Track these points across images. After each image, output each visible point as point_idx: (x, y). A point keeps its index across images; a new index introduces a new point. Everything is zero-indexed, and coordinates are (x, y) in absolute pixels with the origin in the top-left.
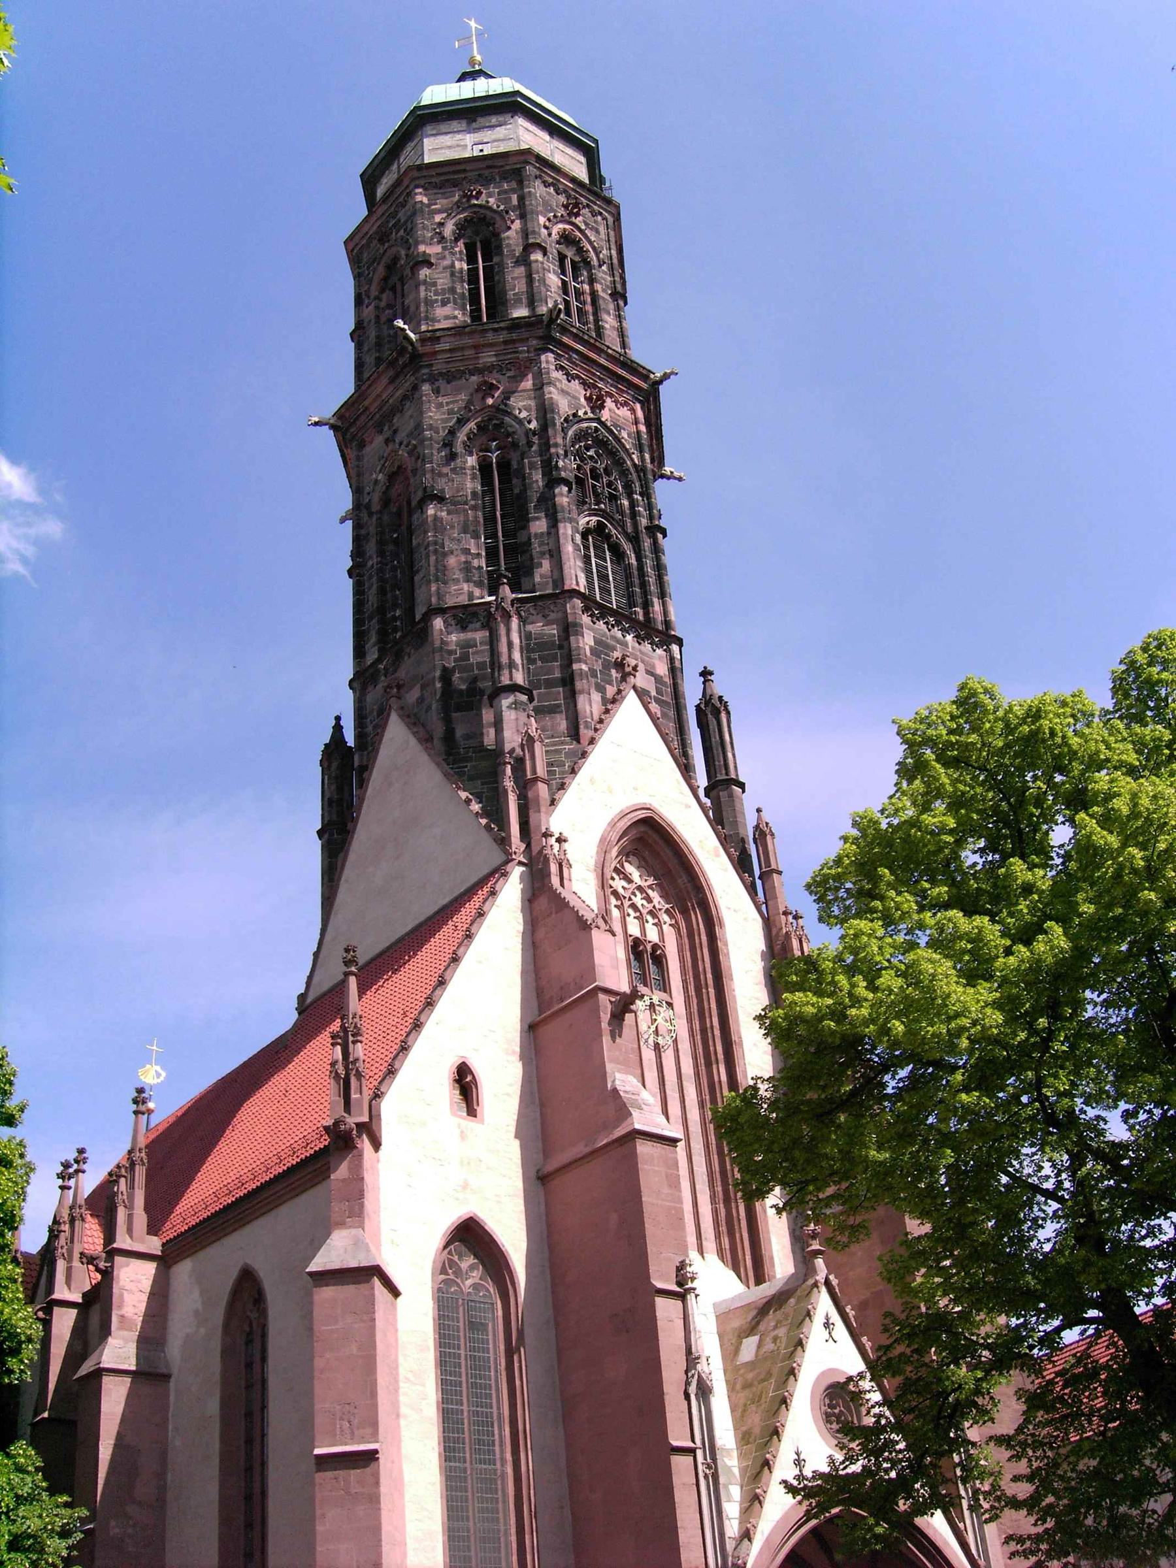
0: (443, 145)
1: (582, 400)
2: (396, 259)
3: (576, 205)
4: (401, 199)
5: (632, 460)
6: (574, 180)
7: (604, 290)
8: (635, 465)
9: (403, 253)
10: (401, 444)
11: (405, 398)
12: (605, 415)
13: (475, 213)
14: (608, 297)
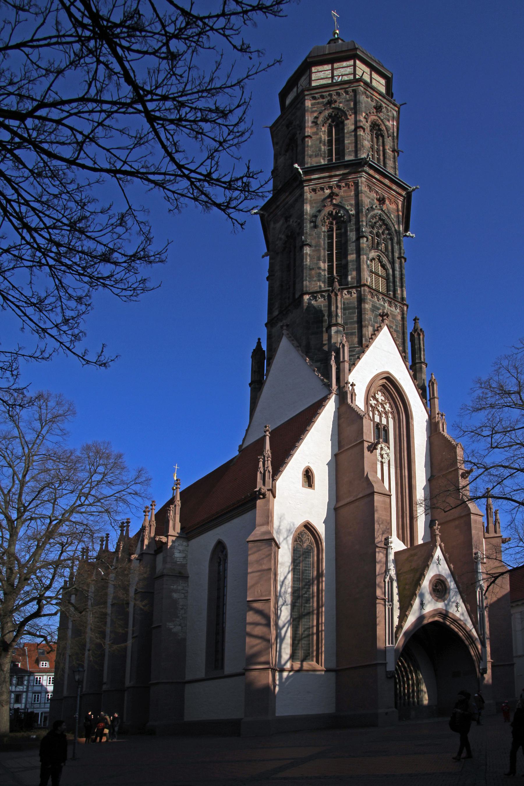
1: (375, 201)
4: (299, 106)
5: (395, 228)
6: (380, 94)
7: (389, 150)
8: (395, 230)
9: (298, 132)
10: (293, 222)
11: (296, 200)
12: (384, 208)
14: (391, 152)
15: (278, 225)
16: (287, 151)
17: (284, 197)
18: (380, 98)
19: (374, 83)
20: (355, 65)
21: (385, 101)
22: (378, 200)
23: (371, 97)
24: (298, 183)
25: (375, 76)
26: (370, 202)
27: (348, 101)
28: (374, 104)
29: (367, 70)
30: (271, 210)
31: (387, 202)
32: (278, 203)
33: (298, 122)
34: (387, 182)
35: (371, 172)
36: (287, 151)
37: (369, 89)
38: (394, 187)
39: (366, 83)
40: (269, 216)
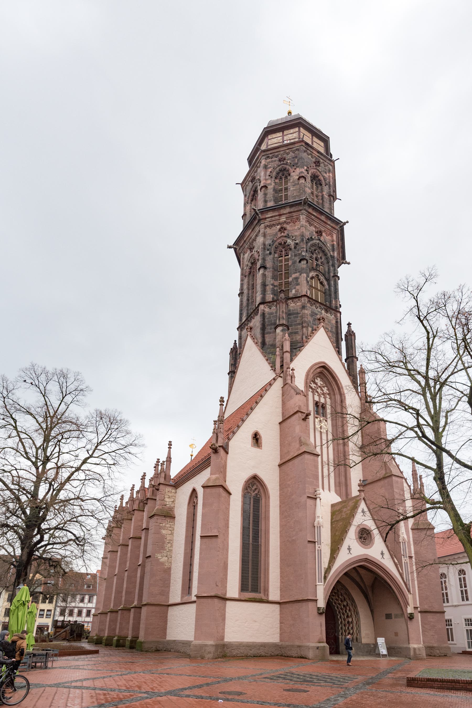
0: (274, 143)
1: (314, 233)
2: (256, 188)
3: (319, 162)
13: (282, 167)
15: (246, 255)
16: (252, 200)
17: (249, 234)
18: (319, 155)
19: (315, 145)
20: (299, 131)
21: (322, 157)
22: (317, 232)
23: (311, 154)
24: (257, 221)
25: (315, 139)
26: (310, 234)
27: (293, 158)
28: (314, 160)
29: (310, 135)
30: (241, 245)
31: (324, 234)
32: (245, 239)
33: (258, 177)
34: (323, 218)
35: (310, 210)
36: (252, 200)
37: (309, 148)
38: (329, 222)
39: (307, 144)
40: (240, 249)
